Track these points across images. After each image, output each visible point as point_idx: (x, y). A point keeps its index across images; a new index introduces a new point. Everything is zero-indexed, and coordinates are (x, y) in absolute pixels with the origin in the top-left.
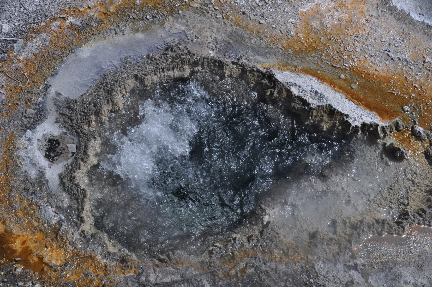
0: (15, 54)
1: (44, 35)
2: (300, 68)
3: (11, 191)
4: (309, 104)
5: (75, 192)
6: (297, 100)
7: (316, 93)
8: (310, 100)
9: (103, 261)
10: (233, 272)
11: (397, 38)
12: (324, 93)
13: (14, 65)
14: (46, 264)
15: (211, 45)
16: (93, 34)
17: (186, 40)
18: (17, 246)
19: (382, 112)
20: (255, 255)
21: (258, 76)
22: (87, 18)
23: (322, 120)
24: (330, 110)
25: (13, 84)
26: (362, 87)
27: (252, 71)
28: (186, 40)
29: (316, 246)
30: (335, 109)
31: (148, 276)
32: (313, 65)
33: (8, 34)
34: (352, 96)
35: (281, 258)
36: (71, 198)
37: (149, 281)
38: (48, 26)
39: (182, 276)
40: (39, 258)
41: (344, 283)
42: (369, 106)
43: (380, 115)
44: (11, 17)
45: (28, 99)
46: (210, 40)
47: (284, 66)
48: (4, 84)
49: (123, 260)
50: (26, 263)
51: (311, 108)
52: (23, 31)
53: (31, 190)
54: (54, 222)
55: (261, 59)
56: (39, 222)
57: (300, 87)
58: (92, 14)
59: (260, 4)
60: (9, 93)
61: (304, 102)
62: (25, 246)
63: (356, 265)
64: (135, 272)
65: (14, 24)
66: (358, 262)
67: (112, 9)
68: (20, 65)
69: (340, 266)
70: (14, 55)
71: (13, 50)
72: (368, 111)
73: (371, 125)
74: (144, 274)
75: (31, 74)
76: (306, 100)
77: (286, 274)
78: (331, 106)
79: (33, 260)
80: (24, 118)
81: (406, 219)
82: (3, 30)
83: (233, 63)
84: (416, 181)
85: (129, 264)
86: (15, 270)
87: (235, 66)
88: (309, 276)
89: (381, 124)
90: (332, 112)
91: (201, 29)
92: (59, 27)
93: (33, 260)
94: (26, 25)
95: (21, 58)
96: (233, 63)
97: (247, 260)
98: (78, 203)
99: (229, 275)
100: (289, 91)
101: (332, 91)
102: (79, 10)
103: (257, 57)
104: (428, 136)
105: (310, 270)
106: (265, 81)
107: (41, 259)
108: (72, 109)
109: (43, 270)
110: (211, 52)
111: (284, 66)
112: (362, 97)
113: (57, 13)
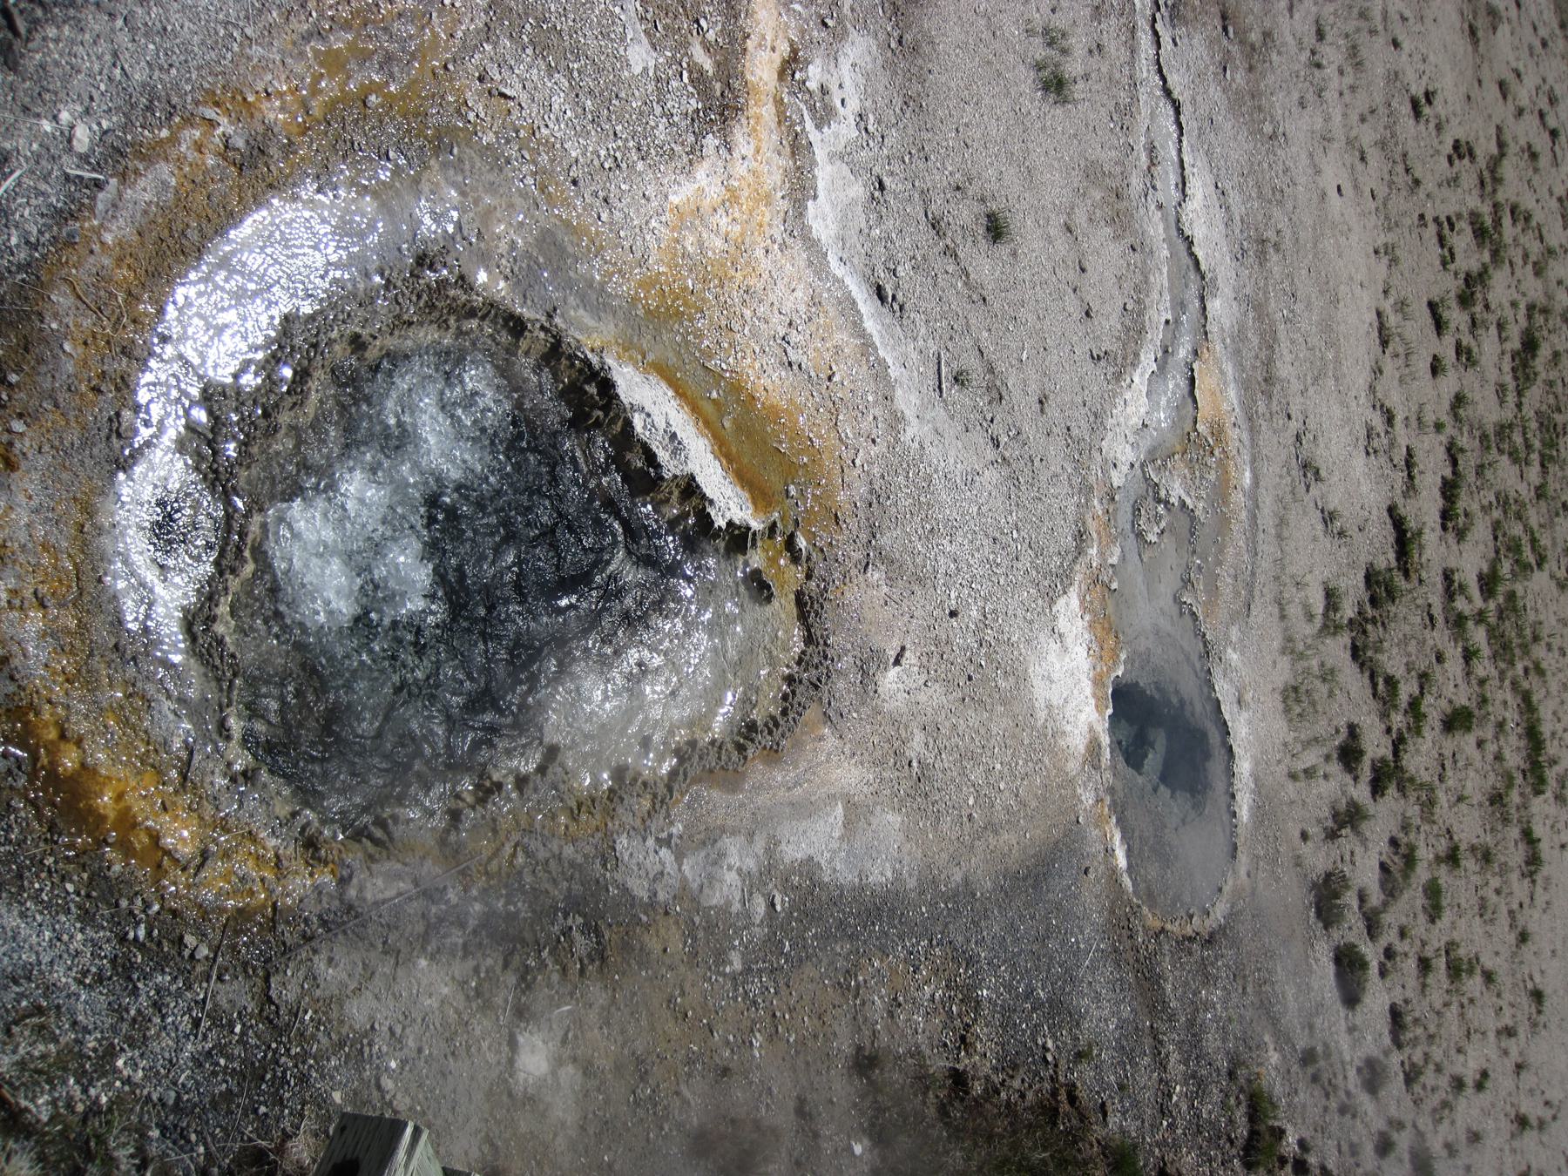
0: (96, 223)
1: (164, 170)
2: (650, 357)
3: (91, 655)
4: (658, 466)
5: (218, 662)
6: (638, 447)
7: (674, 436)
8: (663, 456)
9: (273, 842)
10: (494, 866)
11: (802, 308)
12: (685, 442)
13: (91, 260)
14: (168, 853)
15: (504, 261)
16: (271, 186)
17: (458, 238)
18: (106, 801)
19: (760, 495)
20: (531, 825)
21: (581, 371)
22: (261, 129)
23: (667, 500)
24: (689, 485)
25: (87, 323)
26: (739, 427)
27: (572, 357)
28: (458, 238)
29: (622, 799)
30: (698, 487)
31: (361, 889)
32: (671, 355)
33: (84, 158)
34: (723, 451)
35: (567, 827)
36: (206, 675)
37: (364, 900)
38: (174, 140)
39: (416, 883)
40: (151, 837)
41: (651, 876)
42: (744, 478)
43: (755, 503)
44: (92, 98)
45: (122, 378)
46: (503, 247)
47: (626, 350)
48: (70, 320)
49: (310, 844)
50: (125, 848)
51: (662, 478)
52: (119, 151)
53: (128, 655)
54: (177, 744)
55: (589, 321)
56: (148, 743)
57: (649, 415)
58: (272, 116)
59: (607, 166)
60: (81, 349)
61: (650, 457)
62: (122, 805)
63: (670, 836)
64: (332, 872)
65: (99, 124)
66: (674, 831)
67: (316, 112)
68: (106, 262)
69: (651, 842)
70: (93, 227)
71: (92, 209)
72: (738, 489)
73: (739, 527)
74: (355, 881)
75: (130, 294)
76: (655, 455)
77: (572, 864)
78: (692, 478)
79: (140, 842)
80: (114, 436)
81: (752, 740)
82: (75, 142)
83: (542, 328)
84: (775, 653)
85: (323, 852)
86: (109, 868)
87: (542, 335)
88: (604, 866)
89: (756, 525)
90: (690, 488)
91: (490, 210)
92: (199, 147)
93: (140, 842)
94: (124, 129)
95: (108, 238)
96: (542, 328)
97: (515, 837)
98: (221, 690)
99: (487, 873)
100: (628, 424)
101: (694, 430)
102: (245, 99)
103: (581, 312)
104: (808, 559)
105: (608, 856)
106: (592, 389)
107: (155, 838)
108: (217, 419)
109: (159, 866)
110: (502, 284)
111: (626, 350)
112: (734, 450)
113: (197, 103)
